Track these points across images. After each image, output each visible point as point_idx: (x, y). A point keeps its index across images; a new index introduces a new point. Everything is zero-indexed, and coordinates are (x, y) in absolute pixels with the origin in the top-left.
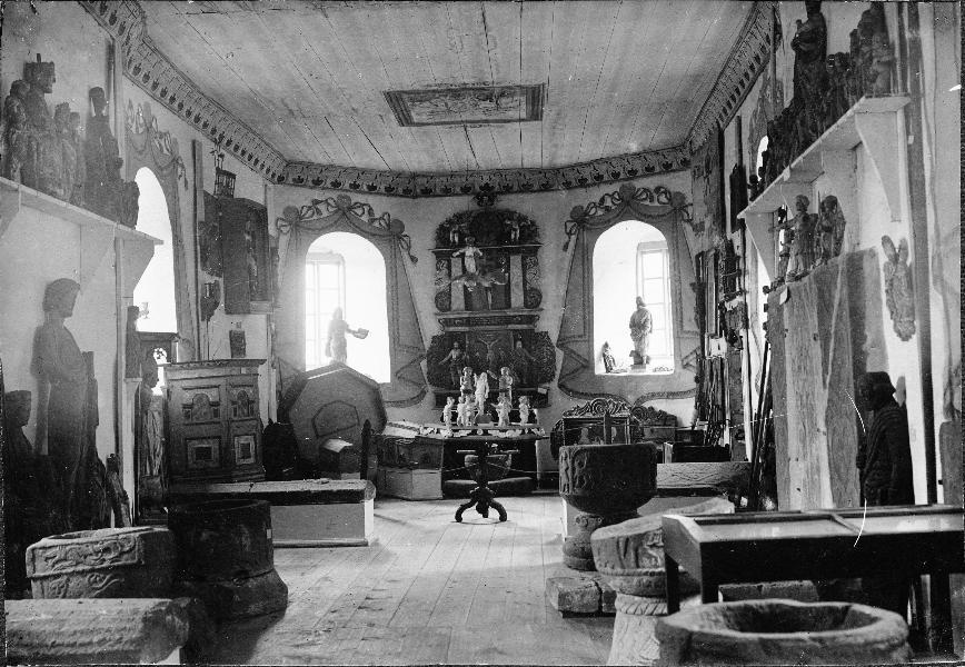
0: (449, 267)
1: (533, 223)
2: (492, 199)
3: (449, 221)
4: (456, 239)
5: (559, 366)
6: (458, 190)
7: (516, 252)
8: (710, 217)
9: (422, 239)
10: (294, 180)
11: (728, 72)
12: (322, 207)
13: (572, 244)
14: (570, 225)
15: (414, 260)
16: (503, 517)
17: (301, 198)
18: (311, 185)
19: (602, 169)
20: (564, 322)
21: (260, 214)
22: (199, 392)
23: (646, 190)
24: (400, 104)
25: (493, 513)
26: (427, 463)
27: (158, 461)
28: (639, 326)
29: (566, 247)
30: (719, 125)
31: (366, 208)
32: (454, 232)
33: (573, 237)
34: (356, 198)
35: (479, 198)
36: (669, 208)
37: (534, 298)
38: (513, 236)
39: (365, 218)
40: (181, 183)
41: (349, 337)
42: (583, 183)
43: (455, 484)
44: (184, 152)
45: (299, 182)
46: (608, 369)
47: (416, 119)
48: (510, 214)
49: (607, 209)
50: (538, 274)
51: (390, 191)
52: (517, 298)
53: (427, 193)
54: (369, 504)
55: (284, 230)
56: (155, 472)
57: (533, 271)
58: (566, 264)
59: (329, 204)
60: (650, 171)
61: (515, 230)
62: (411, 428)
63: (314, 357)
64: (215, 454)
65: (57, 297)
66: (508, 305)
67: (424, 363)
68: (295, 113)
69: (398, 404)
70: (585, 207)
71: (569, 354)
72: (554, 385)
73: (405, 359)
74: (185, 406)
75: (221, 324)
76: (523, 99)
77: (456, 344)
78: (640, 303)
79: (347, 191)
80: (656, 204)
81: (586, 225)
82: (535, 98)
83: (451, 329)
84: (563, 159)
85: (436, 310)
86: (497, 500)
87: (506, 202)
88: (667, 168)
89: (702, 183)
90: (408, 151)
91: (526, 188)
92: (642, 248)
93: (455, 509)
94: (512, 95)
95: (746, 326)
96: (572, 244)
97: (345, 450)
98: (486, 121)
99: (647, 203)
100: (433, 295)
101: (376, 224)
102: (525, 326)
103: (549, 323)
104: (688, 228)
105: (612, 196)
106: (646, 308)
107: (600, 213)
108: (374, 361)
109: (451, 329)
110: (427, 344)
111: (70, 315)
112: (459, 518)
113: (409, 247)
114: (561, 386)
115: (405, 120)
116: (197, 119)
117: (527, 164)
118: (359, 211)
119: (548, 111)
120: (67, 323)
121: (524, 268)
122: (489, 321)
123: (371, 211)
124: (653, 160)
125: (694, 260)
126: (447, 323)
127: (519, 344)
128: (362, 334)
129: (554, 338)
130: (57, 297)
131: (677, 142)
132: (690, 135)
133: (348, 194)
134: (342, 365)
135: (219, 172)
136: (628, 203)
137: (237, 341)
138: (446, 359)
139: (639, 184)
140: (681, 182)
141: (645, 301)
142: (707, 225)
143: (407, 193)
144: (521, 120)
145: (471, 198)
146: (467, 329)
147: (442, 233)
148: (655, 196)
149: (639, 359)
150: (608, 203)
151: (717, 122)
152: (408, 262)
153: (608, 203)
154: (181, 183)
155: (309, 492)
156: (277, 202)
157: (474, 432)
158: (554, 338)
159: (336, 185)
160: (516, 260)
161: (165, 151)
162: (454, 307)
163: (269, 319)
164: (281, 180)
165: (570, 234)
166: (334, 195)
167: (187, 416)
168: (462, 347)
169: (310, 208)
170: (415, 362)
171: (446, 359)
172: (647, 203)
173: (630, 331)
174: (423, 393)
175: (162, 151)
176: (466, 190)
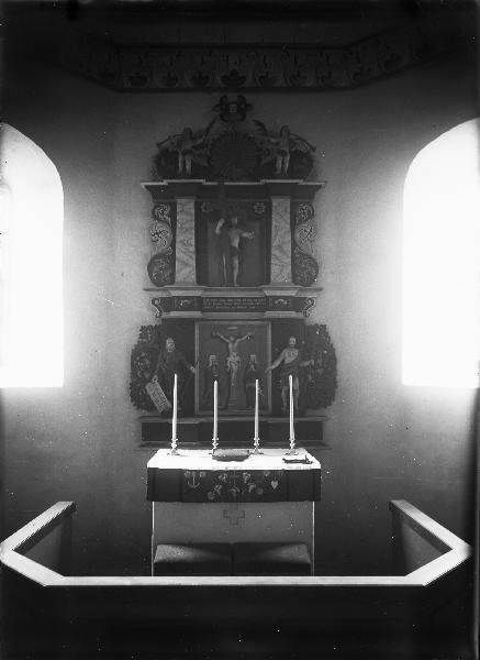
0: (173, 215)
4: (188, 167)
7: (281, 191)
32: (185, 153)
57: (306, 226)
61: (283, 154)
83: (174, 314)
102: (293, 314)
109: (174, 314)
121: (294, 224)
122: (232, 305)
126: (166, 304)
146: (197, 314)
160: (281, 209)
162: (179, 277)
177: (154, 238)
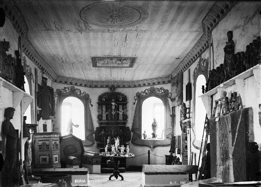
0: (102, 108)
1: (126, 96)
2: (115, 88)
3: (102, 95)
5: (132, 138)
6: (105, 86)
7: (121, 104)
8: (177, 97)
9: (94, 100)
10: (59, 81)
11: (187, 56)
12: (67, 89)
13: (136, 103)
14: (136, 97)
15: (92, 105)
16: (122, 179)
17: (61, 86)
18: (64, 83)
19: (145, 82)
20: (133, 124)
21: (51, 90)
22: (43, 142)
23: (157, 89)
24: (95, 61)
25: (119, 178)
26: (97, 163)
27: (30, 162)
28: (154, 126)
29: (134, 104)
30: (182, 71)
31: (79, 90)
32: (104, 98)
33: (137, 101)
34: (76, 87)
35: (111, 88)
36: (164, 94)
37: (125, 117)
38: (120, 100)
39: (79, 93)
40: (32, 80)
41: (73, 127)
42: (140, 86)
43: (104, 169)
44: (33, 72)
45: (61, 82)
46: (145, 138)
47: (98, 65)
48: (119, 94)
49: (146, 93)
50: (127, 111)
51: (86, 86)
52: (121, 117)
53: (96, 87)
54: (88, 175)
55: (56, 95)
56: (30, 165)
58: (134, 108)
59: (68, 89)
60: (159, 83)
62: (92, 153)
63: (64, 132)
64: (48, 160)
65: (9, 113)
66: (118, 119)
67: (94, 135)
68: (64, 62)
69: (87, 146)
70: (140, 93)
71: (134, 133)
72: (130, 142)
73: (89, 133)
74: (39, 146)
75: (41, 122)
76: (130, 61)
77: (103, 130)
78: (154, 120)
79: (73, 85)
80: (160, 92)
81: (140, 98)
82: (133, 61)
83: (102, 125)
84: (135, 79)
85: (98, 120)
86: (121, 174)
87: (119, 90)
88: (164, 83)
89: (175, 88)
90: (93, 74)
91: (124, 87)
92: (155, 105)
93: (109, 176)
94: (127, 60)
95: (190, 127)
96: (136, 103)
97: (74, 159)
98: (118, 67)
99: (158, 92)
100: (97, 116)
101: (82, 95)
102: (123, 125)
103: (129, 125)
104: (169, 100)
105: (148, 90)
106: (156, 121)
107: (144, 94)
108: (80, 134)
109: (102, 125)
110: (95, 130)
111: (12, 118)
112: (110, 179)
113: (90, 102)
114: (131, 142)
115: (95, 65)
116: (37, 62)
117: (125, 80)
118: (77, 91)
119: (135, 65)
120: (11, 121)
122: (112, 124)
123: (80, 91)
124: (160, 80)
125: (171, 109)
126: (101, 124)
127: (121, 130)
128: (77, 126)
129: (131, 128)
130: (9, 113)
131: (167, 76)
132: (171, 74)
133: (74, 86)
134: (71, 135)
135: (43, 78)
136: (152, 92)
137: (45, 126)
138: (100, 134)
139: (156, 87)
140: (168, 87)
141: (156, 119)
142: (177, 99)
143: (90, 86)
144: (127, 67)
145: (108, 88)
147: (100, 98)
148: (160, 90)
149: (154, 136)
150: (147, 91)
151: (182, 70)
152: (90, 106)
153: (147, 91)
154: (32, 80)
155: (72, 171)
156: (57, 87)
157: (116, 155)
158: (131, 130)
159: (71, 83)
161: (29, 71)
162: (103, 119)
163: (52, 121)
164: (56, 81)
165: (135, 100)
166: (70, 86)
167: (40, 148)
168: (105, 130)
169: (63, 90)
170: (91, 135)
171: (100, 134)
172: (158, 92)
173: (152, 127)
174: (94, 143)
175: (28, 70)
176: (107, 86)
177: (98, 111)
